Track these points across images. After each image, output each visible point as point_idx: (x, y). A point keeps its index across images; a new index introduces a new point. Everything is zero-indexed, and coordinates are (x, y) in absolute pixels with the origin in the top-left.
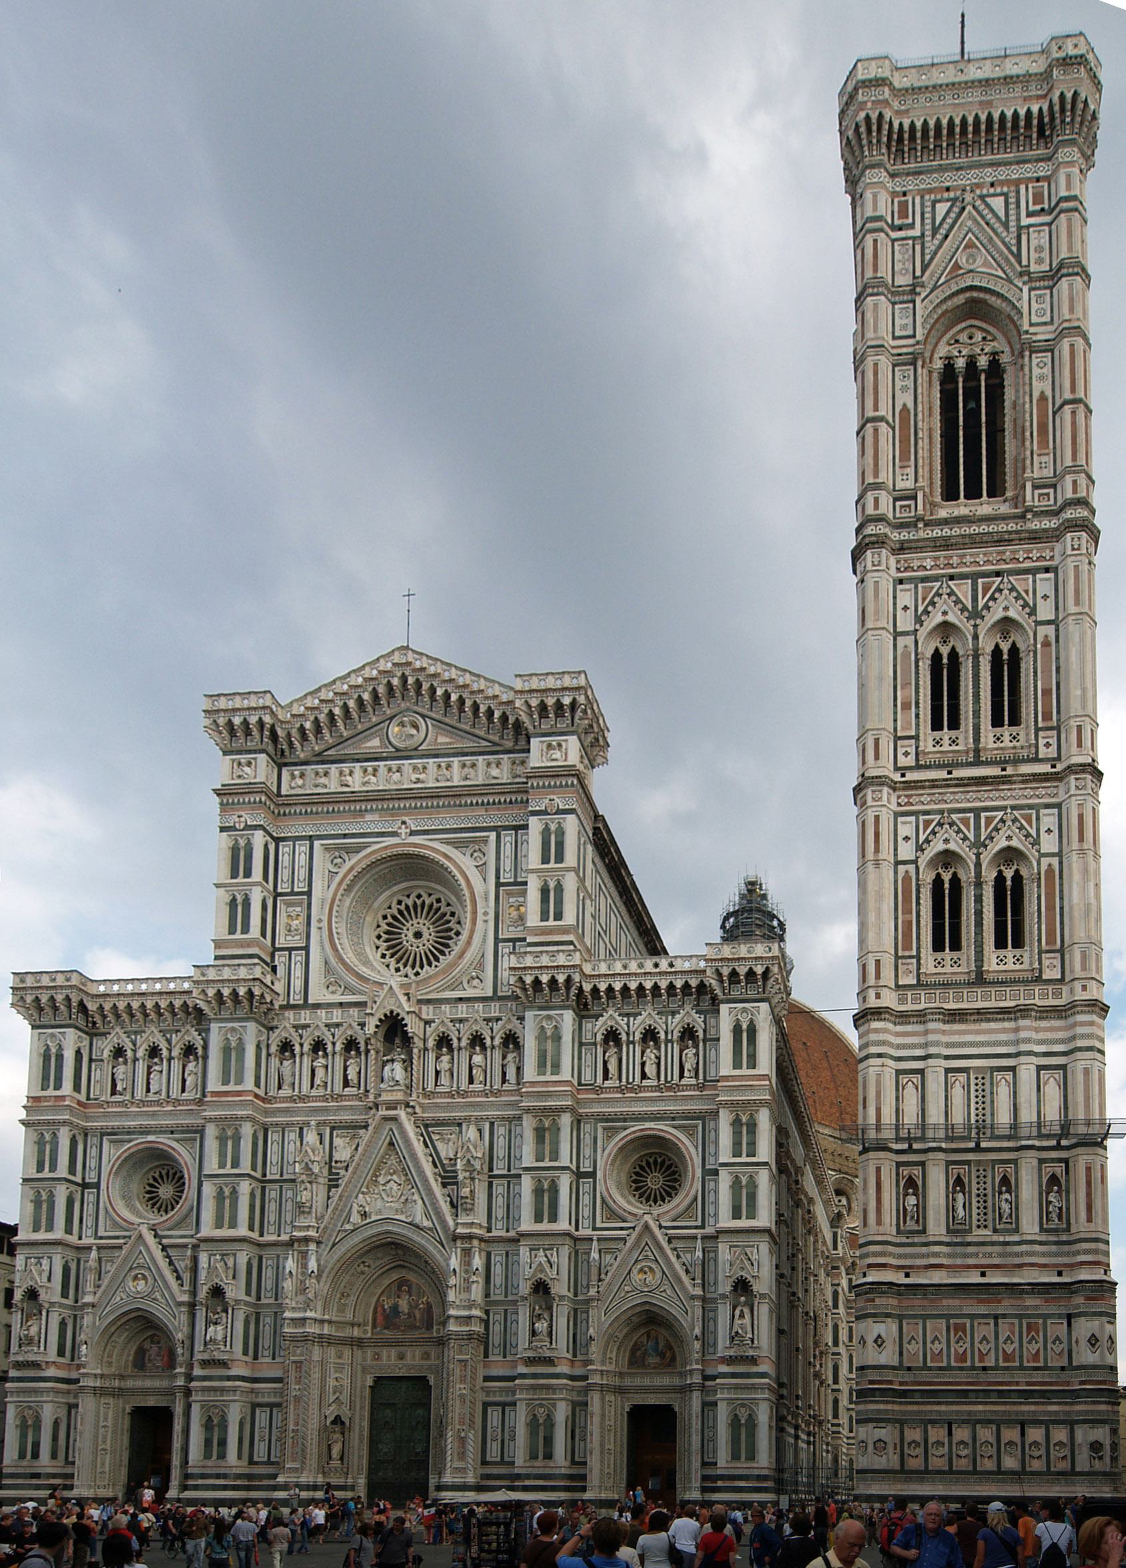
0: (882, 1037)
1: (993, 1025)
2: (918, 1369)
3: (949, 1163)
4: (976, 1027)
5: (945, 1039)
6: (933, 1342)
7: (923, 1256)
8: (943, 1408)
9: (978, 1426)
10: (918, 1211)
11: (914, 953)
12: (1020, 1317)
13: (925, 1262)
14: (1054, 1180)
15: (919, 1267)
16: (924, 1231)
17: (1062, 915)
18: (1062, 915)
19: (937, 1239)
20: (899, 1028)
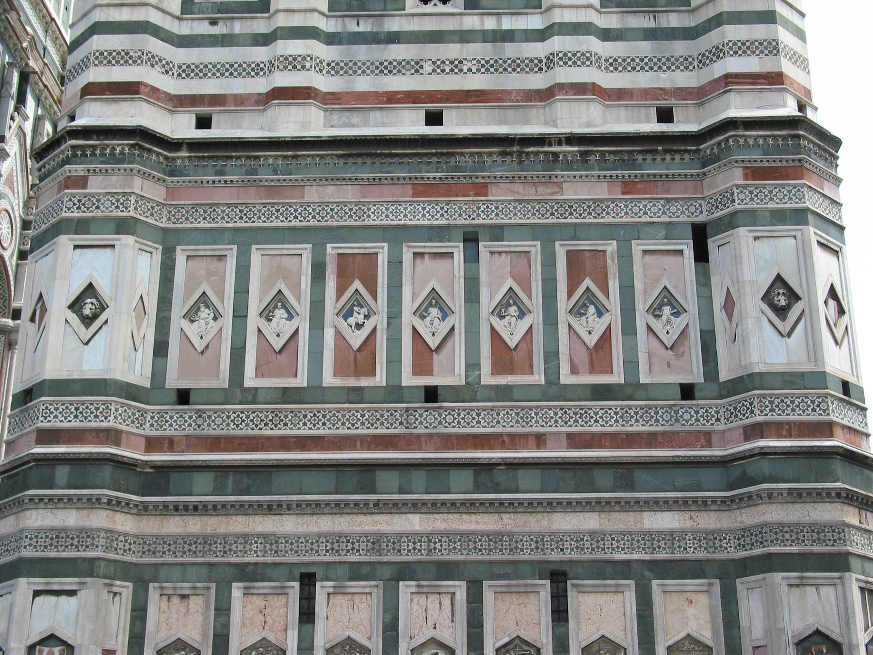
6: (267, 314)
7: (257, 70)
8: (289, 525)
9: (406, 588)
13: (260, 85)
15: (240, 100)
19: (297, 21)
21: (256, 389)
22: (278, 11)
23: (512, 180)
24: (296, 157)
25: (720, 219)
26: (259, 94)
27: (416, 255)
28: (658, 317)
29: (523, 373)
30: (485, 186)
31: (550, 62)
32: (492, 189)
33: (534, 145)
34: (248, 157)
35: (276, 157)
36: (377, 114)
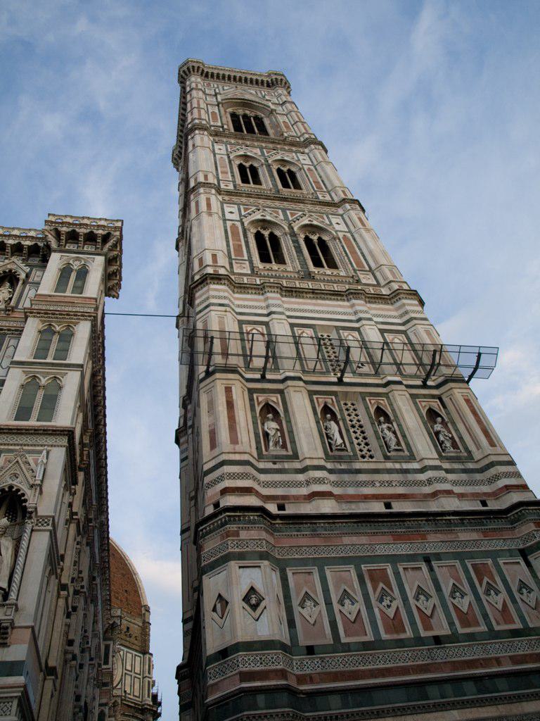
0: (222, 294)
1: (328, 302)
2: (326, 649)
3: (311, 393)
4: (314, 301)
5: (286, 306)
6: (341, 602)
7: (299, 484)
10: (283, 436)
11: (246, 258)
12: (460, 556)
13: (304, 491)
14: (432, 415)
15: (297, 499)
16: (295, 456)
17: (364, 256)
18: (364, 256)
19: (316, 463)
20: (237, 295)
21: (348, 644)
22: (305, 458)
23: (436, 532)
24: (334, 523)
25: (531, 546)
26: (305, 495)
27: (404, 568)
28: (522, 594)
29: (476, 626)
30: (424, 535)
31: (430, 482)
32: (428, 536)
33: (440, 516)
34: (311, 523)
35: (324, 523)
36: (363, 504)
